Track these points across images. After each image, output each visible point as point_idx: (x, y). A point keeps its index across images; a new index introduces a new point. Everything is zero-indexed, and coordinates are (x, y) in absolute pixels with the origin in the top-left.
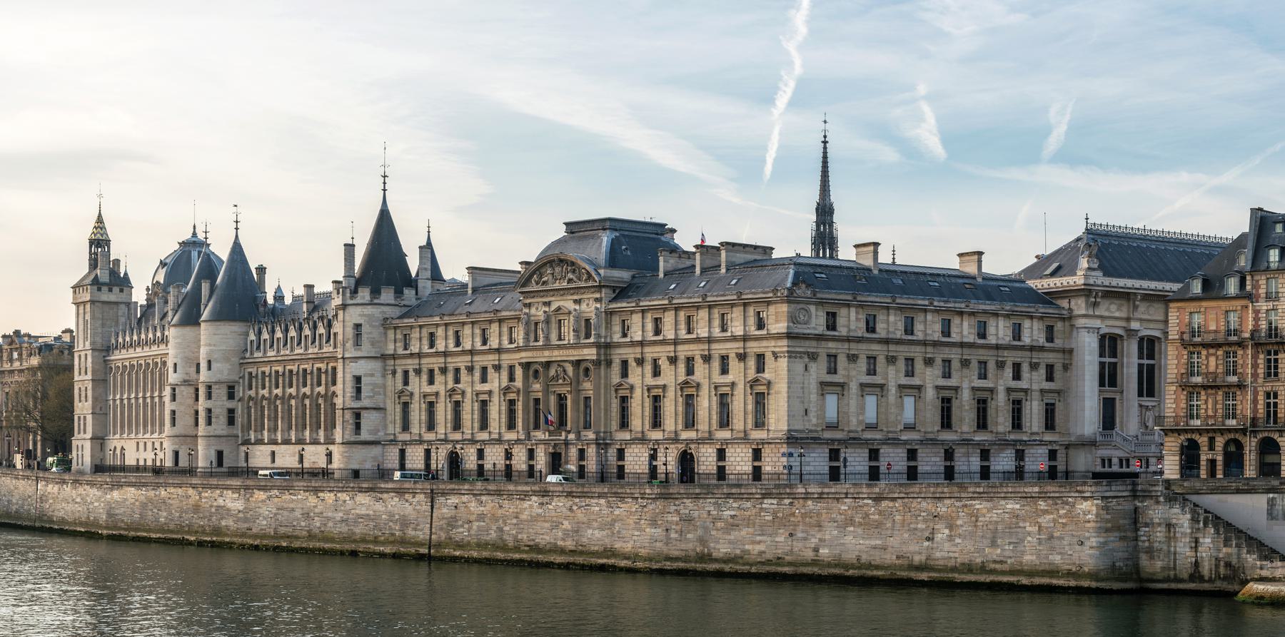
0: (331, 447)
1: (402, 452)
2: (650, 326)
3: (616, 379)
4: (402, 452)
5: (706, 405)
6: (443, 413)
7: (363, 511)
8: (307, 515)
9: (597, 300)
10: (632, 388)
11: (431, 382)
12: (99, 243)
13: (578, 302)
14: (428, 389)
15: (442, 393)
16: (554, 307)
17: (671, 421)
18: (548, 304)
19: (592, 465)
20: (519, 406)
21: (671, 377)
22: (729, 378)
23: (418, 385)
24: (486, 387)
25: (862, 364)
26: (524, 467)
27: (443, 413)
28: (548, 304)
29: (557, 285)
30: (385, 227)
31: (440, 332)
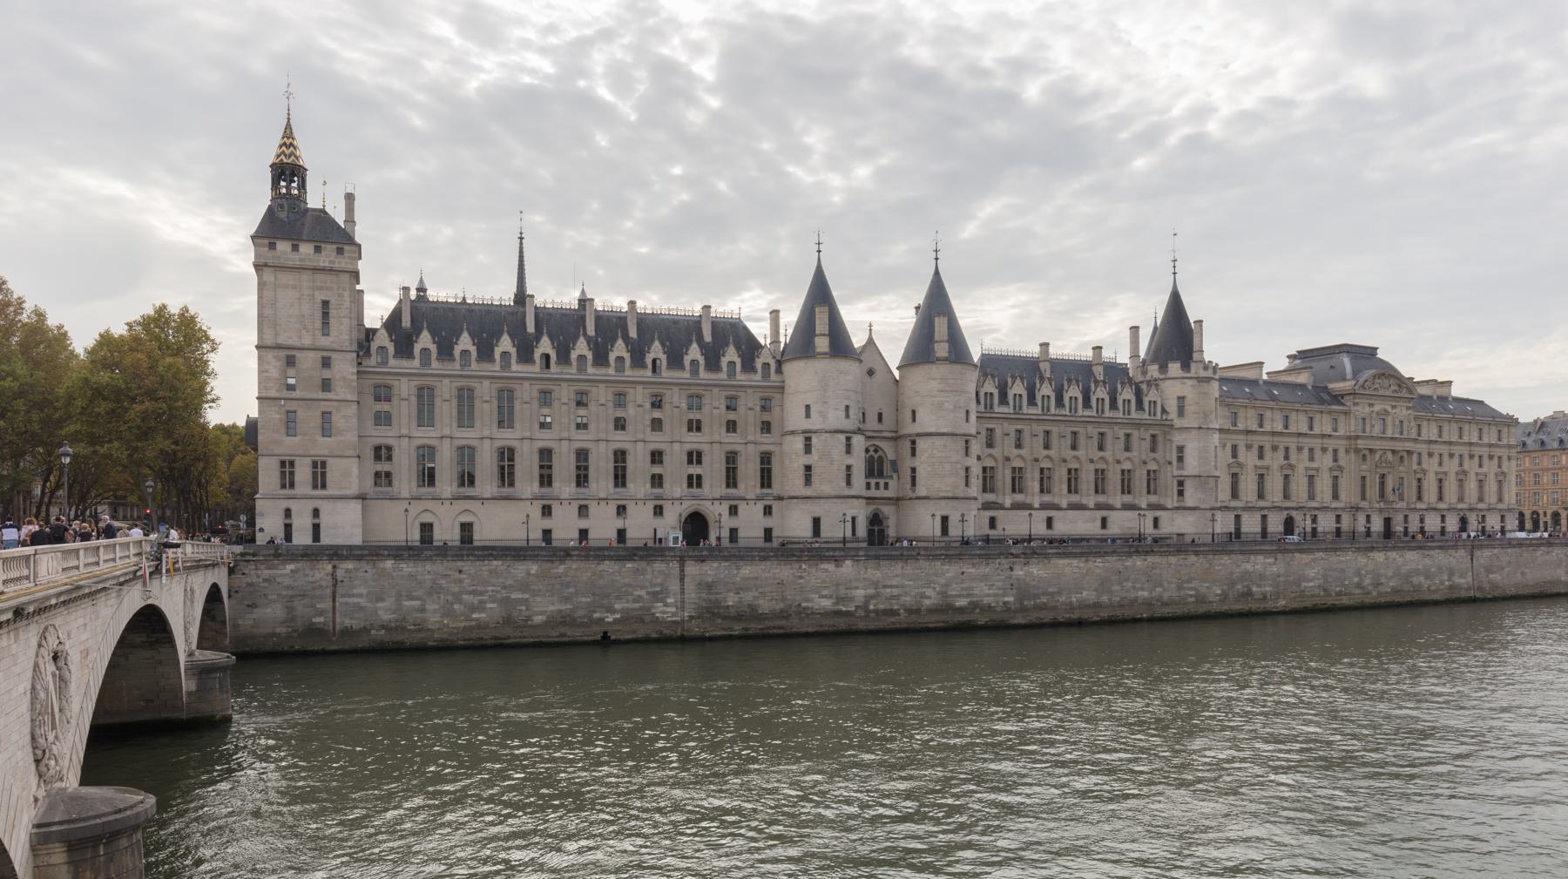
0: (1158, 513)
1: (1238, 517)
2: (1435, 431)
3: (1415, 467)
4: (1238, 517)
5: (1472, 485)
6: (1274, 485)
7: (1413, 566)
8: (1358, 573)
9: (1408, 408)
10: (1424, 472)
11: (1261, 457)
12: (287, 172)
13: (1394, 407)
14: (1259, 463)
15: (1276, 466)
16: (1377, 408)
17: (1451, 494)
18: (1371, 405)
19: (1414, 526)
20: (1343, 482)
21: (1452, 466)
22: (1485, 470)
23: (1249, 459)
24: (1315, 465)
25: (1436, 459)
26: (1363, 529)
27: (1274, 485)
28: (1371, 405)
29: (1381, 392)
30: (1176, 306)
31: (1268, 414)
